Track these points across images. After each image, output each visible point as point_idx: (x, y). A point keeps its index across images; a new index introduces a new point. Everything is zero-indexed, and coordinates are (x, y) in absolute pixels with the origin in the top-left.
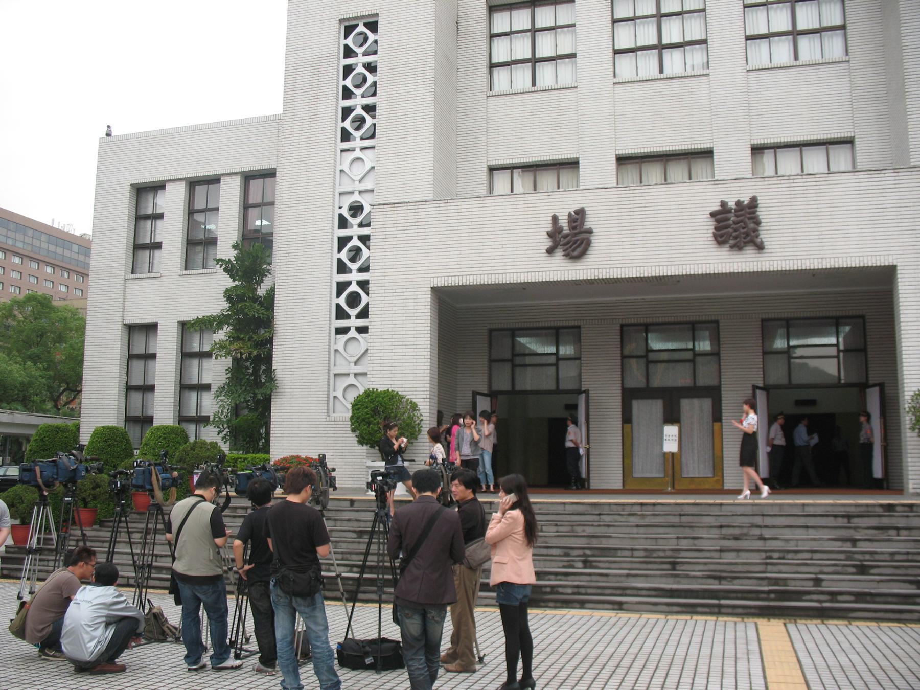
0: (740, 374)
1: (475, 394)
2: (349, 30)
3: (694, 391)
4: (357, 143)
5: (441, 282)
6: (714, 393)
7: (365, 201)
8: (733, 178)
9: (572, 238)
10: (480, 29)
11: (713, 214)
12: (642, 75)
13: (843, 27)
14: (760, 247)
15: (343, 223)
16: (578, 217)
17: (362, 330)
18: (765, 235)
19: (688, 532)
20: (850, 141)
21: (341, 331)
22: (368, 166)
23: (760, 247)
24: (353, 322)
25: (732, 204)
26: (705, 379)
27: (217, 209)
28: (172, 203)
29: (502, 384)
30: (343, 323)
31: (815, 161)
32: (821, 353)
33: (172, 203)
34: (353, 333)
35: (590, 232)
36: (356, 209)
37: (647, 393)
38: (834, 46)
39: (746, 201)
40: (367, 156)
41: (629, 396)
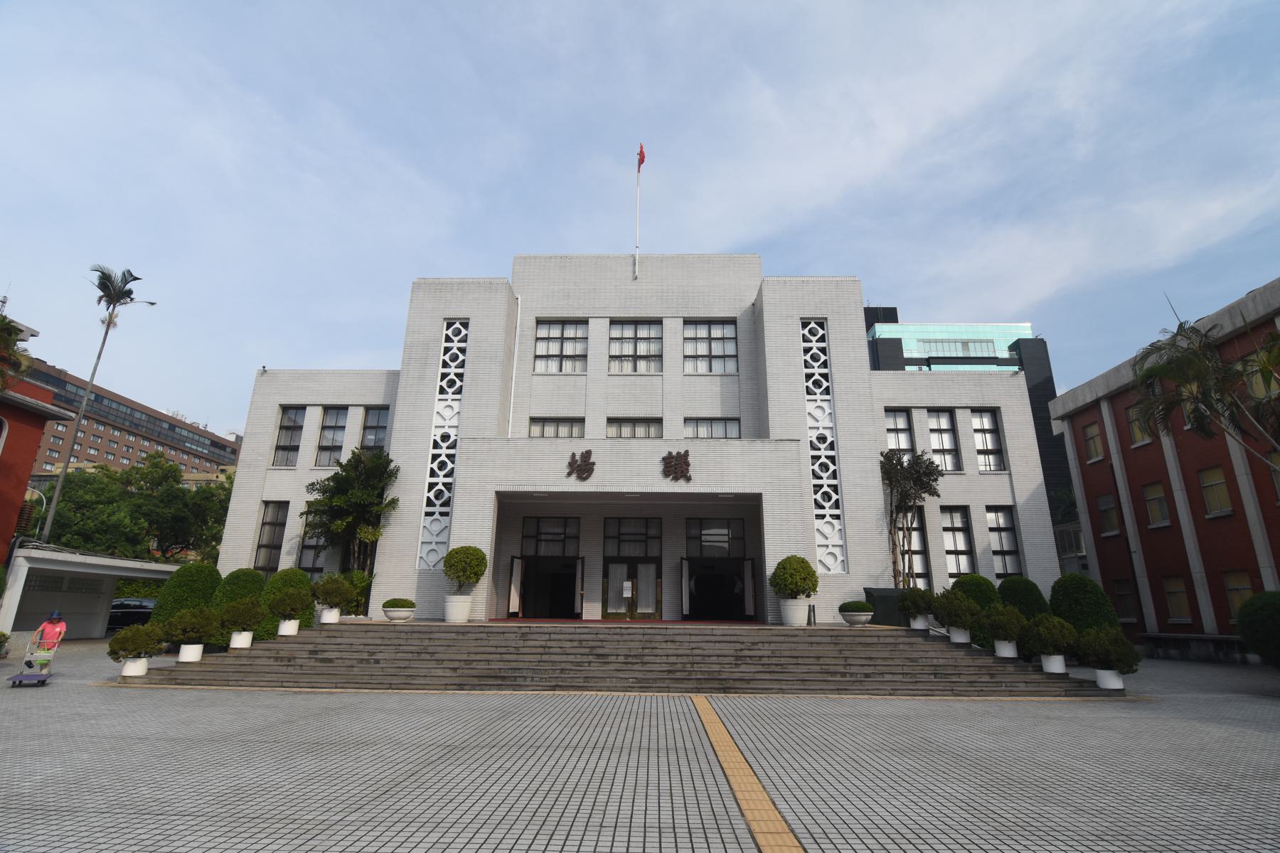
0: (674, 551)
1: (513, 558)
2: (448, 327)
3: (646, 560)
4: (450, 396)
5: (502, 489)
6: (658, 561)
7: (452, 432)
8: (676, 437)
11: (664, 459)
12: (625, 372)
13: (736, 356)
14: (688, 479)
15: (436, 445)
16: (587, 454)
17: (442, 514)
18: (692, 472)
19: (649, 645)
20: (738, 420)
21: (427, 514)
22: (456, 410)
23: (688, 479)
24: (437, 509)
25: (674, 454)
26: (653, 552)
27: (344, 427)
28: (312, 420)
29: (531, 552)
30: (430, 509)
31: (718, 429)
32: (717, 537)
33: (312, 420)
34: (437, 516)
35: (594, 464)
36: (445, 437)
37: (619, 560)
38: (731, 366)
39: (683, 452)
40: (455, 404)
41: (608, 561)
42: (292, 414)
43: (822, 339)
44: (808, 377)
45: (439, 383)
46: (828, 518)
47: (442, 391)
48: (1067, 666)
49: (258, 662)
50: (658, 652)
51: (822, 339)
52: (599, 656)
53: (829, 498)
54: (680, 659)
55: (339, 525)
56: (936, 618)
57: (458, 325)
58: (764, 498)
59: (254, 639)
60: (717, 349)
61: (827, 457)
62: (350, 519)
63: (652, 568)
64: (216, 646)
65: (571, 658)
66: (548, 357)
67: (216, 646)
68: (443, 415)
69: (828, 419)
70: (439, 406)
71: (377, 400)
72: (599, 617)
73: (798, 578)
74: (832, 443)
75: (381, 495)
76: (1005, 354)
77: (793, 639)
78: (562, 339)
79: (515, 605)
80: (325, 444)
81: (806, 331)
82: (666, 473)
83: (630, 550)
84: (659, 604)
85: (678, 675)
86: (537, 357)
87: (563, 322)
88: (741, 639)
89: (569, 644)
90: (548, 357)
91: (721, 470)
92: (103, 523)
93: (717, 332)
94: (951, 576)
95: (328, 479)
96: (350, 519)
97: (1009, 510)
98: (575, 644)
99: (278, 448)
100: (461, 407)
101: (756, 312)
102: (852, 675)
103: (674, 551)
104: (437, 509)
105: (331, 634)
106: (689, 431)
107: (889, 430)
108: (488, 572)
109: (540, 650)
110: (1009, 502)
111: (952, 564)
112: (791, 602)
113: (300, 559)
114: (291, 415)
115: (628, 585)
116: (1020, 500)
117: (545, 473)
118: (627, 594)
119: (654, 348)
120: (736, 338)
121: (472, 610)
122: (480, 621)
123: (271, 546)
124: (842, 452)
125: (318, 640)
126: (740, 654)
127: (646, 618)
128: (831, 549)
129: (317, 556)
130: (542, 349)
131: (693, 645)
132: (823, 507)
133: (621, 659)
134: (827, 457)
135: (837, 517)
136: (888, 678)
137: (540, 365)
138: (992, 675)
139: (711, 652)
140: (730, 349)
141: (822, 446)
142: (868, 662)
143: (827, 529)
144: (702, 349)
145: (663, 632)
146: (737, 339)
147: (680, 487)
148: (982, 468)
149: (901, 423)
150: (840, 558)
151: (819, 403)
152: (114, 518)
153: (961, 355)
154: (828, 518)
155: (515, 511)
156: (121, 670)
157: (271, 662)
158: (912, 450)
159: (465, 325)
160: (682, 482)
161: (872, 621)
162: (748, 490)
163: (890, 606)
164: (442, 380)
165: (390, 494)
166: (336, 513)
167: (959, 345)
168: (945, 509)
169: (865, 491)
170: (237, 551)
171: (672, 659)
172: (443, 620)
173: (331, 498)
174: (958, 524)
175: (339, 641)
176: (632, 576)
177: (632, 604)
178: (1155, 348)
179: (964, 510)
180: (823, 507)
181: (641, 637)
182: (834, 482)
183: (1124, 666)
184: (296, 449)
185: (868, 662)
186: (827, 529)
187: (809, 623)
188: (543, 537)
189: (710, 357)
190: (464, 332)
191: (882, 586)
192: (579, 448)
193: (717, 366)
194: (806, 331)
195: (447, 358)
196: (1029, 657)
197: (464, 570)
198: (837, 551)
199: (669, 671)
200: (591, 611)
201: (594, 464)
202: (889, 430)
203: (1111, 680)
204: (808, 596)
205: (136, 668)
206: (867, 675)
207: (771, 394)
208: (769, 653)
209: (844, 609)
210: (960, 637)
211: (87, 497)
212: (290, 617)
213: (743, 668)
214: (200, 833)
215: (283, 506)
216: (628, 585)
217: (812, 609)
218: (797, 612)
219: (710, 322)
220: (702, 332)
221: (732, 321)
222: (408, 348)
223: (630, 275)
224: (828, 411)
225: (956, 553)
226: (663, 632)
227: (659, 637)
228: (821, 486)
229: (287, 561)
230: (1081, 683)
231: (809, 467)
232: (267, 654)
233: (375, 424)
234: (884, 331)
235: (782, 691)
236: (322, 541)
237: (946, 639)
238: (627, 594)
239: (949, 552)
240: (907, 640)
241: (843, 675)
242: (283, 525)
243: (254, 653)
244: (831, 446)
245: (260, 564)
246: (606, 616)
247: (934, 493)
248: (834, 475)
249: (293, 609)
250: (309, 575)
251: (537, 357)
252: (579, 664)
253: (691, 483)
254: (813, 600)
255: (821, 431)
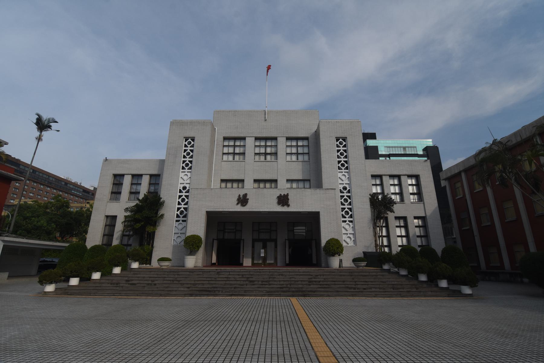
0: (282, 237)
3: (271, 240)
4: (187, 170)
6: (275, 241)
7: (187, 186)
8: (283, 187)
9: (243, 200)
10: (221, 143)
11: (278, 197)
12: (261, 160)
13: (308, 153)
14: (288, 206)
15: (180, 191)
16: (245, 195)
17: (183, 221)
18: (290, 203)
20: (309, 180)
21: (177, 221)
22: (189, 176)
23: (288, 206)
24: (181, 219)
27: (141, 184)
28: (127, 181)
30: (178, 219)
31: (301, 185)
32: (300, 230)
33: (127, 181)
34: (181, 222)
35: (248, 199)
36: (184, 188)
37: (259, 240)
38: (306, 158)
39: (286, 194)
40: (189, 174)
41: (254, 241)
42: (118, 178)
43: (345, 146)
44: (339, 162)
45: (182, 165)
46: (347, 222)
47: (183, 168)
48: (448, 284)
49: (104, 285)
50: (276, 279)
51: (345, 146)
52: (251, 281)
53: (348, 214)
54: (285, 283)
55: (138, 225)
56: (393, 264)
57: (190, 140)
58: (320, 213)
59: (102, 276)
60: (300, 150)
61: (347, 196)
62: (143, 223)
63: (273, 244)
64: (85, 278)
65: (238, 282)
66: (228, 154)
67: (85, 278)
68: (184, 178)
69: (347, 180)
70: (182, 175)
71: (155, 172)
72: (250, 265)
73: (335, 247)
74: (349, 190)
75: (157, 213)
76: (421, 153)
77: (333, 274)
78: (235, 146)
79: (214, 260)
80: (132, 191)
81: (338, 143)
82: (279, 203)
83: (263, 236)
84: (276, 259)
85: (284, 289)
86: (224, 154)
87: (235, 139)
88: (311, 274)
89: (238, 276)
90: (228, 154)
91: (303, 202)
92: (35, 225)
93: (300, 143)
94: (399, 246)
95: (134, 206)
96: (143, 223)
97: (423, 219)
98: (240, 276)
99: (112, 193)
100: (191, 175)
101: (317, 134)
102: (358, 288)
103: (282, 237)
104: (181, 219)
105: (135, 273)
106: (288, 185)
107: (373, 185)
108: (203, 246)
109: (226, 279)
110: (423, 215)
111: (399, 241)
112: (332, 258)
113: (121, 241)
114: (118, 179)
115: (263, 251)
116: (428, 214)
117: (227, 203)
118: (262, 255)
119: (273, 150)
120: (308, 146)
121: (196, 262)
122: (200, 267)
123: (109, 235)
124: (354, 194)
125: (130, 276)
126: (311, 280)
127: (270, 265)
128: (349, 235)
129: (129, 239)
130: (226, 150)
131: (291, 277)
132: (345, 218)
133: (260, 283)
134: (347, 196)
135: (351, 222)
136: (373, 290)
137: (225, 157)
138: (417, 288)
139: (299, 279)
140: (306, 150)
141: (345, 191)
142: (365, 283)
143: (347, 227)
144: (294, 150)
145: (278, 271)
146: (310, 146)
147: (285, 209)
148: (412, 201)
149: (378, 182)
150: (353, 239)
151: (344, 173)
152: (39, 223)
153: (403, 153)
154: (347, 222)
155: (214, 219)
156: (44, 289)
157: (109, 285)
158: (383, 193)
159: (193, 140)
160: (286, 207)
161: (366, 266)
162: (314, 210)
163: (374, 259)
164: (183, 163)
165: (161, 212)
166: (136, 221)
167: (402, 149)
168: (396, 218)
169: (363, 210)
170: (94, 237)
171: (282, 283)
172: (184, 267)
173: (134, 215)
174: (402, 224)
175: (138, 276)
176: (264, 247)
177: (265, 259)
178: (484, 150)
179: (405, 219)
180: (345, 218)
181: (268, 273)
182: (350, 207)
183: (472, 284)
184: (120, 193)
185: (365, 283)
186: (347, 227)
187: (340, 267)
188: (226, 231)
189: (297, 154)
190: (192, 143)
191: (370, 251)
192: (242, 192)
193: (301, 158)
194: (338, 143)
195: (185, 154)
196: (433, 280)
197: (193, 245)
198: (351, 236)
199: (281, 288)
200: (247, 262)
201: (248, 199)
202: (373, 185)
203: (467, 290)
204: (339, 255)
205: (50, 288)
206: (364, 289)
207: (323, 170)
208: (323, 280)
209: (355, 260)
210: (403, 272)
211: (28, 215)
212: (117, 266)
213: (312, 286)
214: (79, 360)
215: (114, 218)
216: (263, 251)
217: (341, 261)
218: (335, 262)
219: (297, 139)
220: (294, 143)
221: (306, 139)
222: (168, 149)
223: (263, 119)
224: (347, 177)
225: (401, 236)
226: (278, 271)
227: (276, 273)
228: (345, 208)
229: (115, 242)
230: (454, 291)
231: (340, 201)
232: (107, 281)
233: (154, 182)
234: (371, 143)
235: (328, 296)
236: (131, 233)
237: (398, 273)
238: (262, 255)
239: (398, 236)
240: (381, 274)
241: (354, 289)
242: (114, 226)
243: (102, 281)
244: (349, 192)
245: (104, 243)
246: (253, 264)
247: (392, 211)
248: (350, 204)
249: (118, 262)
250: (126, 247)
251: (224, 154)
252: (242, 285)
253: (290, 207)
254: (341, 257)
255: (344, 185)
